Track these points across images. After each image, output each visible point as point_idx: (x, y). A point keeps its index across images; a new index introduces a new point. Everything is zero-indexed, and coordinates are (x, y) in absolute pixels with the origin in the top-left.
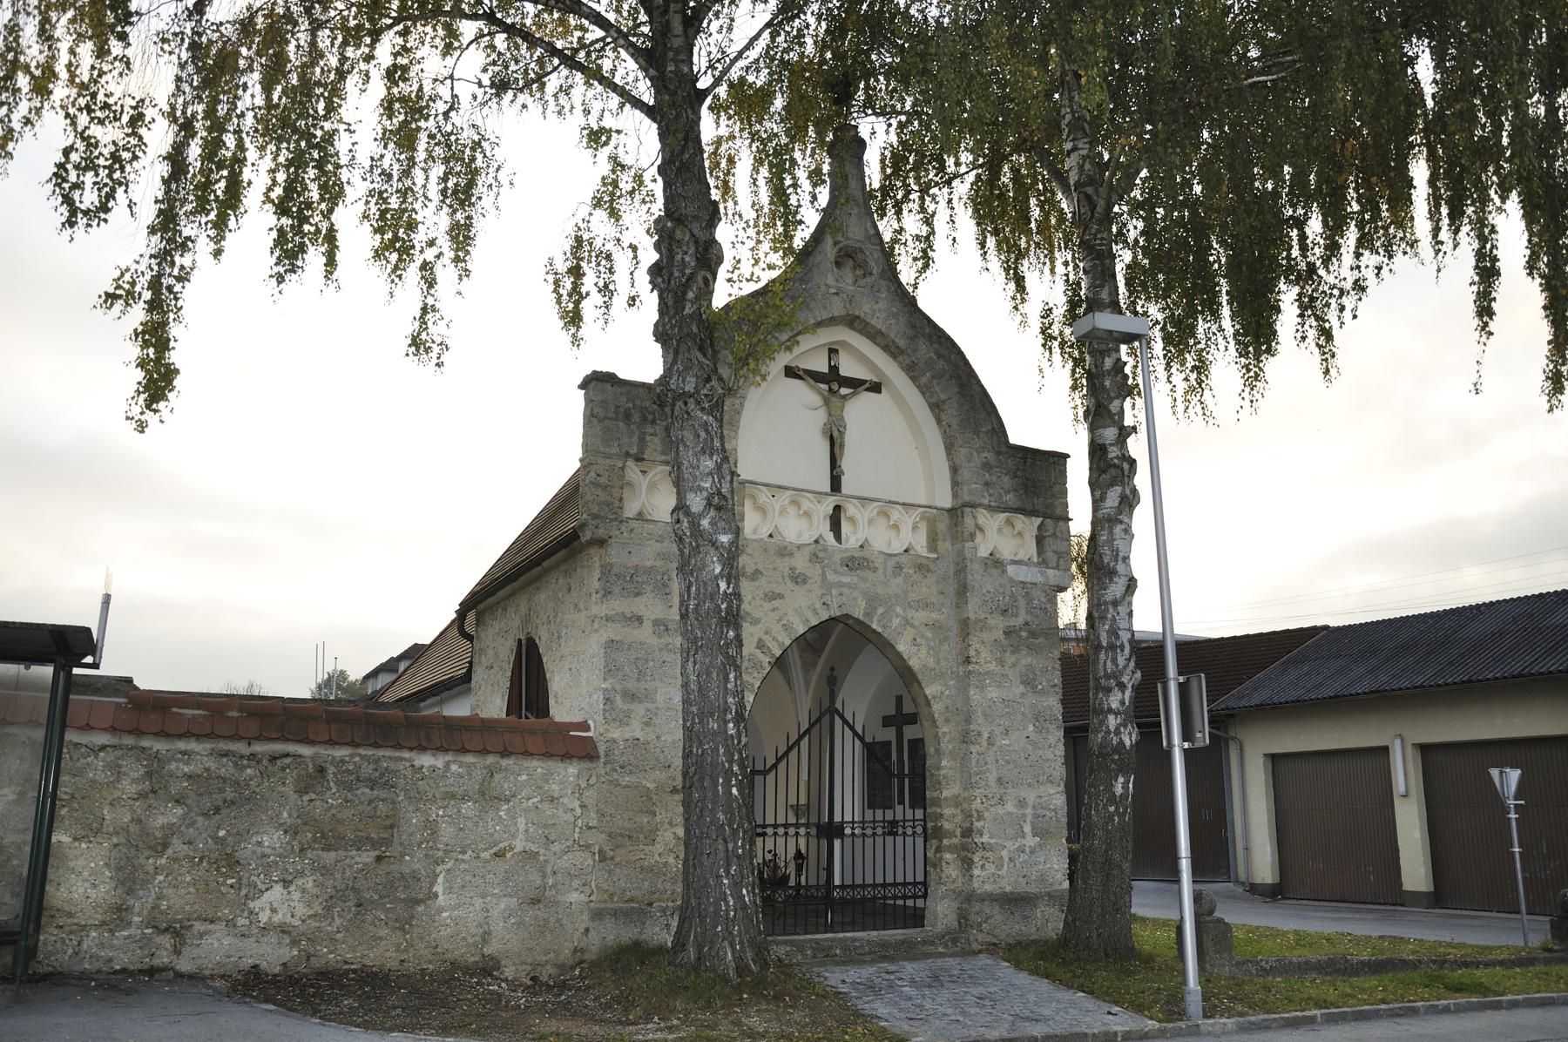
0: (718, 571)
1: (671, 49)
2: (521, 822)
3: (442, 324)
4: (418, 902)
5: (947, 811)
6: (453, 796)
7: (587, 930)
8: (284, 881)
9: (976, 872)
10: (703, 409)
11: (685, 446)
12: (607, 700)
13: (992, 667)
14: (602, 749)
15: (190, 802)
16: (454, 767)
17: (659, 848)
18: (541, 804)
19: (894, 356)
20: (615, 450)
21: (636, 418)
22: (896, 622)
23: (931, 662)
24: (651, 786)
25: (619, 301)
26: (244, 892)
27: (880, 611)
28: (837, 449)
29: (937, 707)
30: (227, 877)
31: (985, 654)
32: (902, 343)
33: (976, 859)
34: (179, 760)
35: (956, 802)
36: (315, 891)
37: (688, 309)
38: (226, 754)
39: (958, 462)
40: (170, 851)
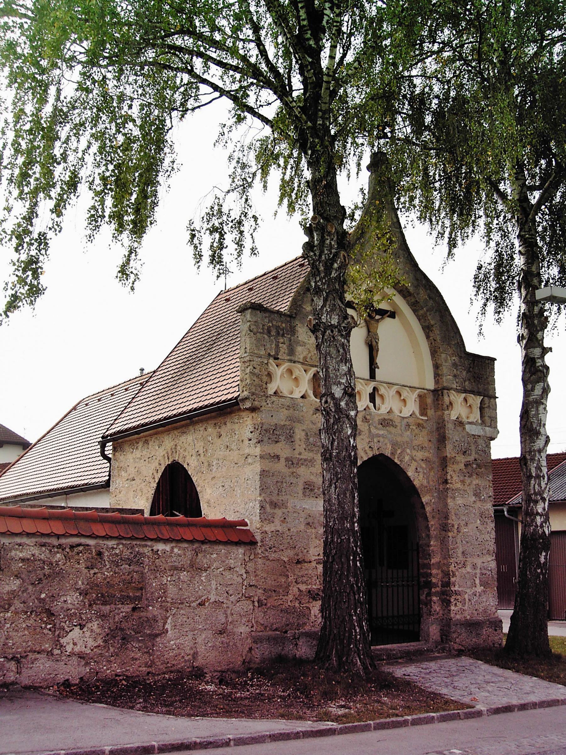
0: (349, 433)
1: (321, 110)
2: (214, 582)
3: (139, 263)
4: (157, 635)
5: (434, 571)
6: (176, 568)
7: (251, 649)
8: (80, 625)
9: (453, 608)
10: (342, 335)
11: (331, 357)
12: (262, 507)
13: (459, 485)
14: (258, 538)
15: (23, 576)
16: (176, 550)
17: (291, 597)
18: (224, 574)
19: (404, 297)
20: (262, 352)
21: (273, 333)
22: (407, 458)
23: (425, 482)
24: (286, 559)
25: (247, 251)
26: (57, 633)
27: (399, 451)
28: (374, 353)
29: (428, 509)
30: (46, 624)
31: (455, 478)
32: (411, 289)
33: (452, 600)
34: (17, 549)
35: (438, 565)
36: (98, 631)
37: (334, 274)
38: (43, 545)
39: (439, 362)
40: (13, 608)
